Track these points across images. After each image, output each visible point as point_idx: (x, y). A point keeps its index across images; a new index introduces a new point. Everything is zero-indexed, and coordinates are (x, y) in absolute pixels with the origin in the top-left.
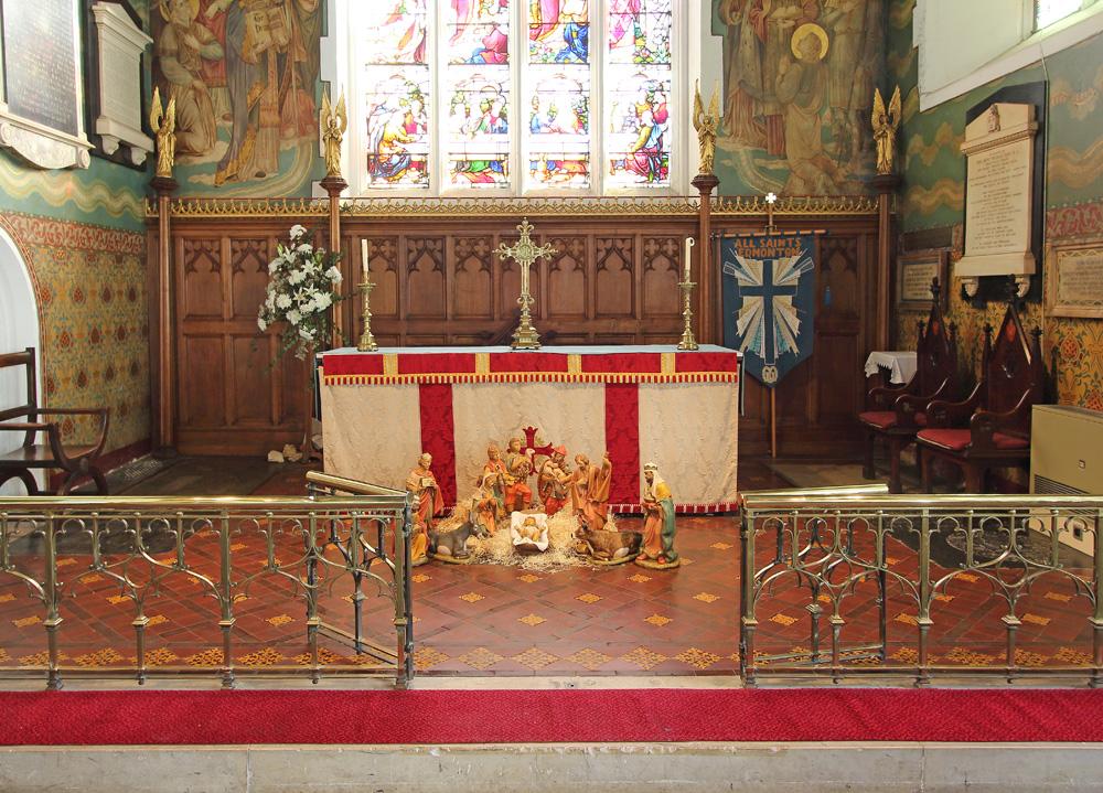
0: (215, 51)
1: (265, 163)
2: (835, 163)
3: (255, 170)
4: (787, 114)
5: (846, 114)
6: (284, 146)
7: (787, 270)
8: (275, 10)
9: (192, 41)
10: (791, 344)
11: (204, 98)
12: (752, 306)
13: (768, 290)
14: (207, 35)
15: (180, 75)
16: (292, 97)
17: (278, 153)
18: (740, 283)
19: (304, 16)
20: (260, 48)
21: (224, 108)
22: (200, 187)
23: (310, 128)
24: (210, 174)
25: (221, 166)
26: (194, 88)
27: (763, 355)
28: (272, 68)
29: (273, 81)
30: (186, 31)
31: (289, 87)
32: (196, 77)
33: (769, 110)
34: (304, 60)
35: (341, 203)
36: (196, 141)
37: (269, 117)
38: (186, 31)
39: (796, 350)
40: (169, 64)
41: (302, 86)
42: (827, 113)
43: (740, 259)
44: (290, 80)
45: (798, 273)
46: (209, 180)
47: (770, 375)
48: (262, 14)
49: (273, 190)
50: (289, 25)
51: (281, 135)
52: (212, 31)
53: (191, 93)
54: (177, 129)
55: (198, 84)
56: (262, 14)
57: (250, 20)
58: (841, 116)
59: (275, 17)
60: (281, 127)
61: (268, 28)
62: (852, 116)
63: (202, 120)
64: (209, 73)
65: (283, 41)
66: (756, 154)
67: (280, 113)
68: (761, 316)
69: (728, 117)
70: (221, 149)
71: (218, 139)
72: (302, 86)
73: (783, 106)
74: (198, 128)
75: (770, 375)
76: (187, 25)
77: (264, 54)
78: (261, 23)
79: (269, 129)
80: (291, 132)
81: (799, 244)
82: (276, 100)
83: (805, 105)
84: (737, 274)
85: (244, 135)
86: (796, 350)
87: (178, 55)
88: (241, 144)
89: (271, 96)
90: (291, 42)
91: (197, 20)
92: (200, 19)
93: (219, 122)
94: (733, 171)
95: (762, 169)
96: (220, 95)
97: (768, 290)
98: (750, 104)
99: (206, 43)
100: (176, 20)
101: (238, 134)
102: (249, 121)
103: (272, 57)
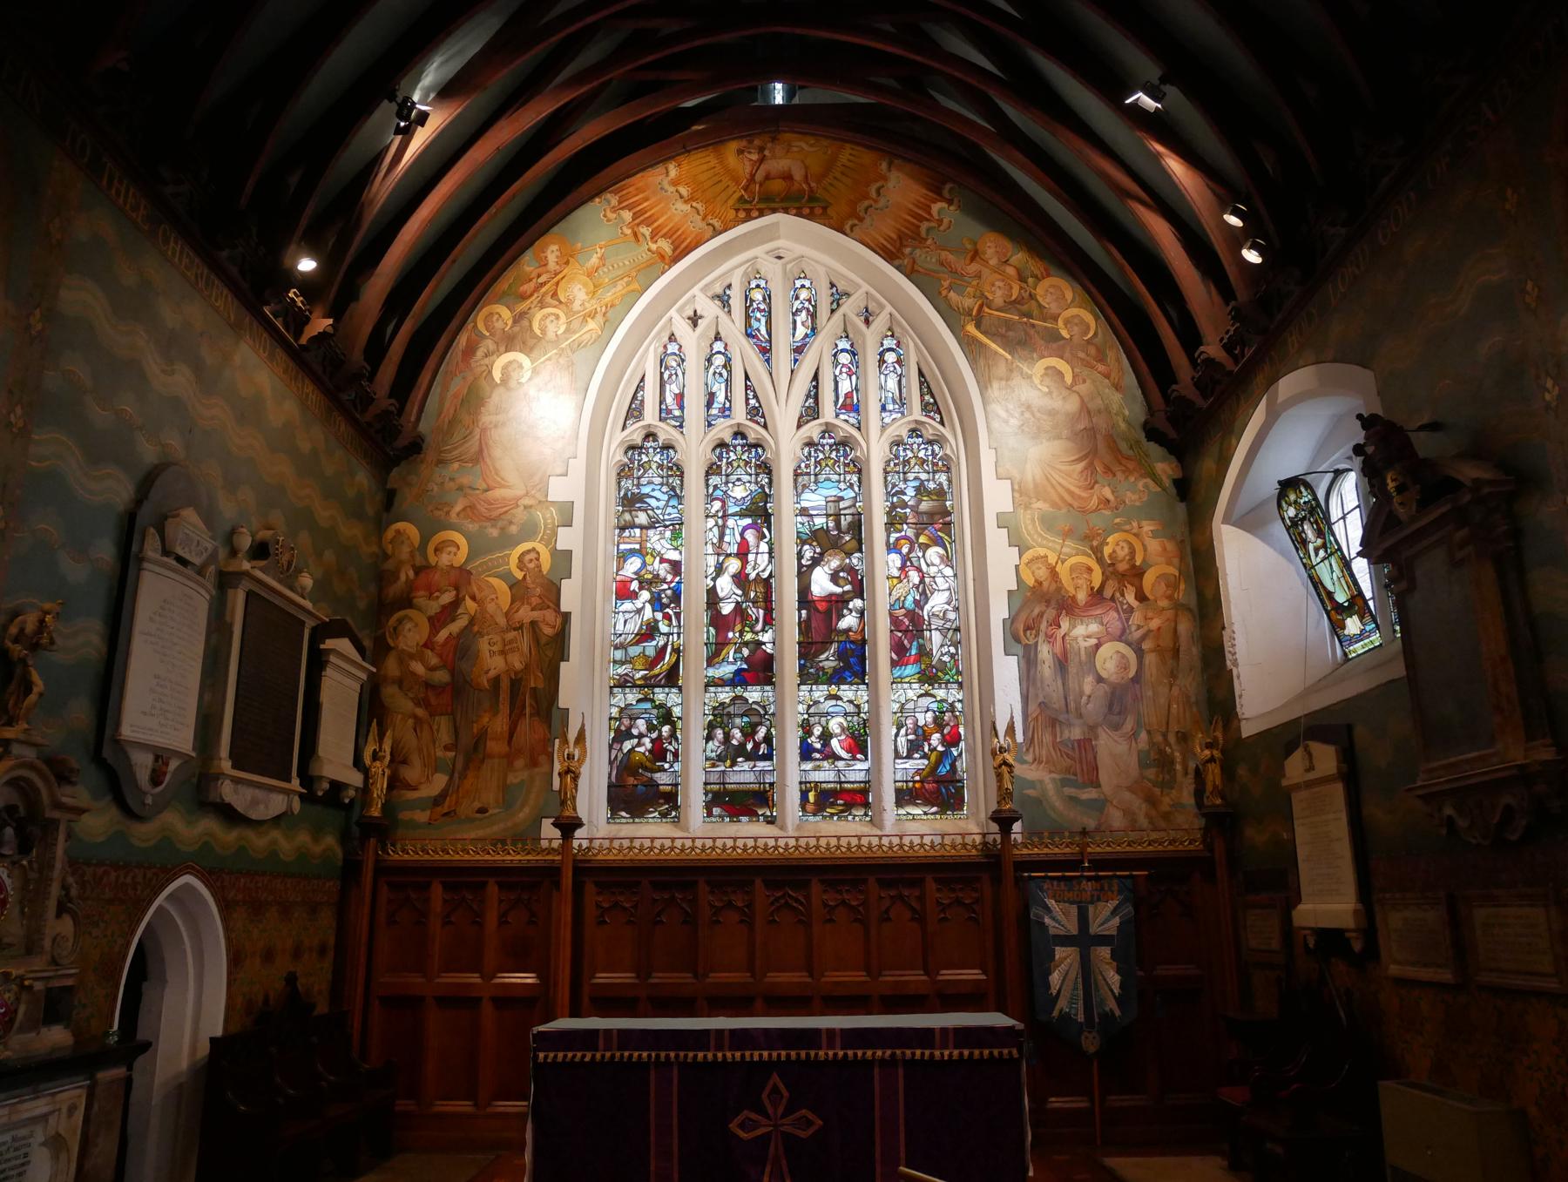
0: (442, 676)
1: (489, 797)
2: (1157, 791)
3: (477, 805)
4: (1096, 738)
5: (1165, 736)
6: (512, 779)
7: (1106, 917)
8: (513, 634)
9: (418, 668)
10: (1112, 1005)
11: (426, 727)
12: (1065, 956)
13: (1084, 940)
14: (434, 661)
15: (401, 703)
16: (524, 726)
17: (505, 788)
18: (1052, 931)
19: (543, 640)
20: (492, 673)
21: (445, 737)
22: (414, 825)
23: (543, 759)
24: (423, 810)
25: (437, 801)
26: (415, 717)
27: (1081, 1018)
28: (504, 695)
29: (504, 708)
30: (412, 657)
31: (522, 714)
32: (418, 704)
33: (1077, 733)
34: (541, 686)
35: (575, 844)
36: (411, 773)
37: (495, 747)
38: (412, 657)
39: (1118, 1013)
40: (390, 692)
41: (537, 712)
42: (1143, 735)
43: (1051, 903)
44: (524, 707)
45: (1116, 921)
46: (422, 816)
47: (1090, 1043)
48: (497, 638)
49: (495, 828)
50: (526, 649)
51: (510, 764)
52: (440, 656)
53: (411, 722)
54: (392, 761)
55: (420, 712)
56: (497, 638)
57: (484, 645)
58: (1159, 738)
59: (511, 642)
60: (509, 758)
61: (503, 652)
62: (1172, 739)
63: (420, 750)
64: (433, 701)
65: (518, 666)
66: (1065, 783)
67: (509, 742)
68: (1076, 965)
69: (1030, 741)
70: (440, 781)
71: (436, 770)
72: (537, 712)
73: (1092, 728)
74: (416, 761)
75: (1090, 1043)
76: (413, 651)
77: (496, 681)
78: (495, 648)
79: (496, 761)
80: (519, 763)
81: (1115, 888)
82: (506, 728)
83: (1116, 727)
84: (1047, 920)
85: (466, 767)
86: (1118, 1013)
87: (400, 682)
88: (463, 776)
89: (500, 724)
90: (527, 667)
91: (426, 645)
92: (428, 645)
93: (440, 753)
94: (1038, 802)
95: (1071, 798)
96: (443, 727)
97: (1084, 940)
98: (1053, 726)
99: (432, 669)
100: (402, 646)
101: (459, 766)
102: (472, 753)
103: (505, 684)
